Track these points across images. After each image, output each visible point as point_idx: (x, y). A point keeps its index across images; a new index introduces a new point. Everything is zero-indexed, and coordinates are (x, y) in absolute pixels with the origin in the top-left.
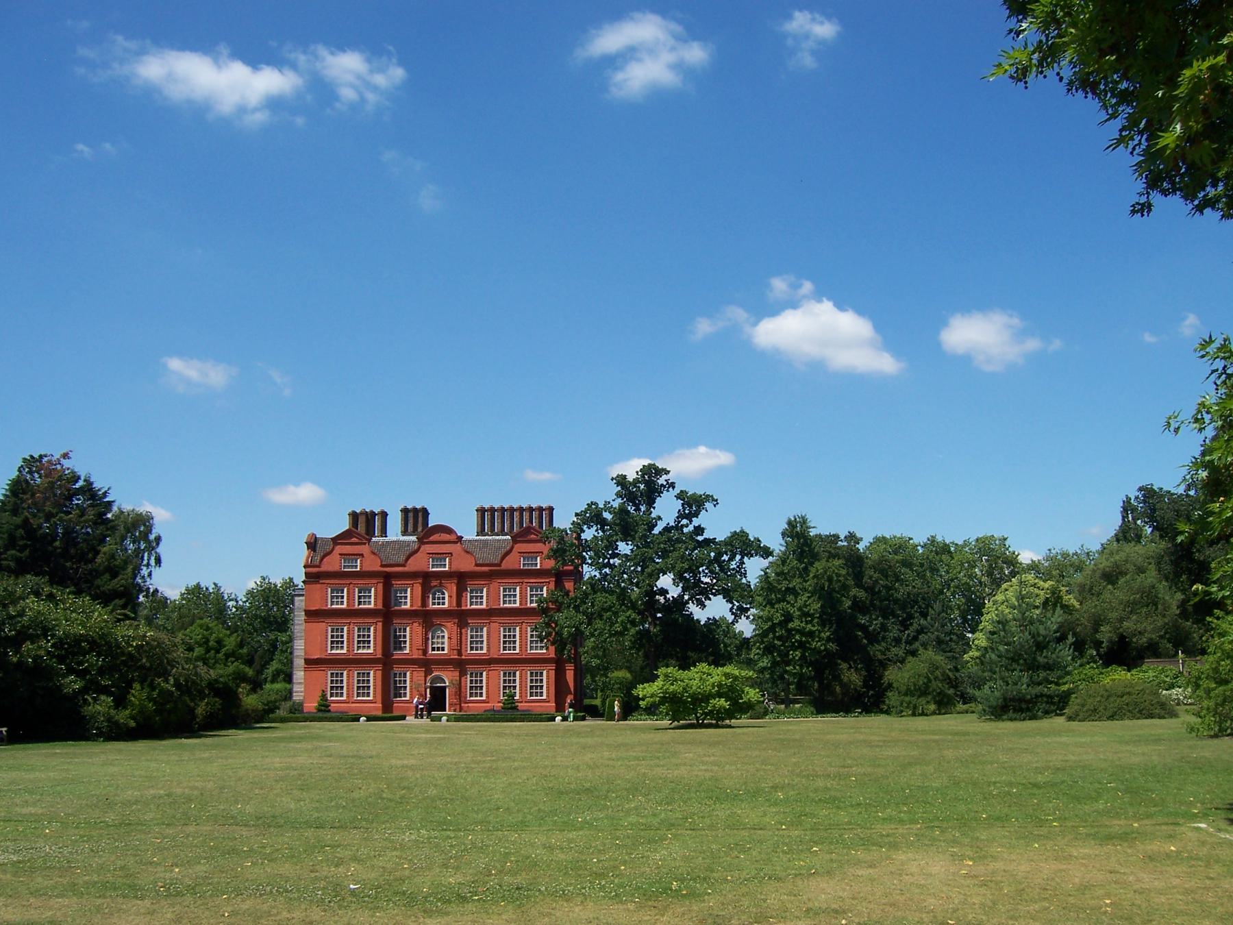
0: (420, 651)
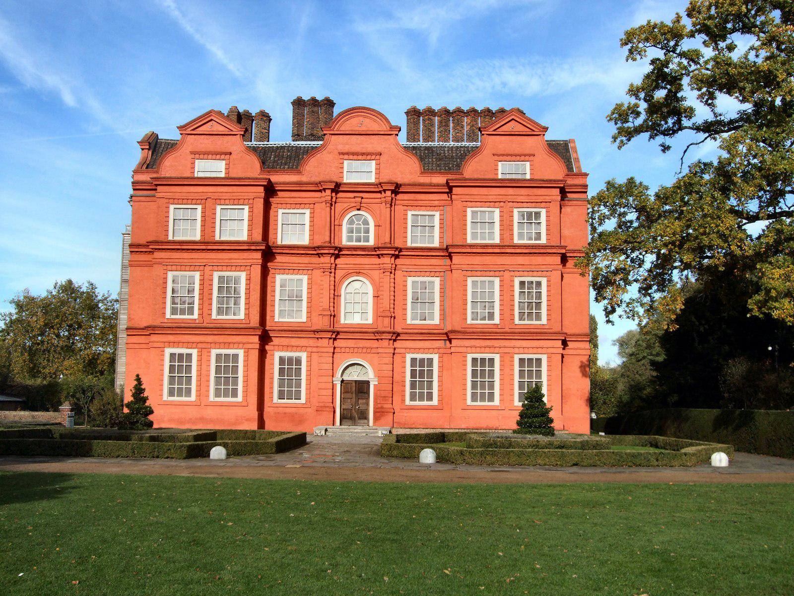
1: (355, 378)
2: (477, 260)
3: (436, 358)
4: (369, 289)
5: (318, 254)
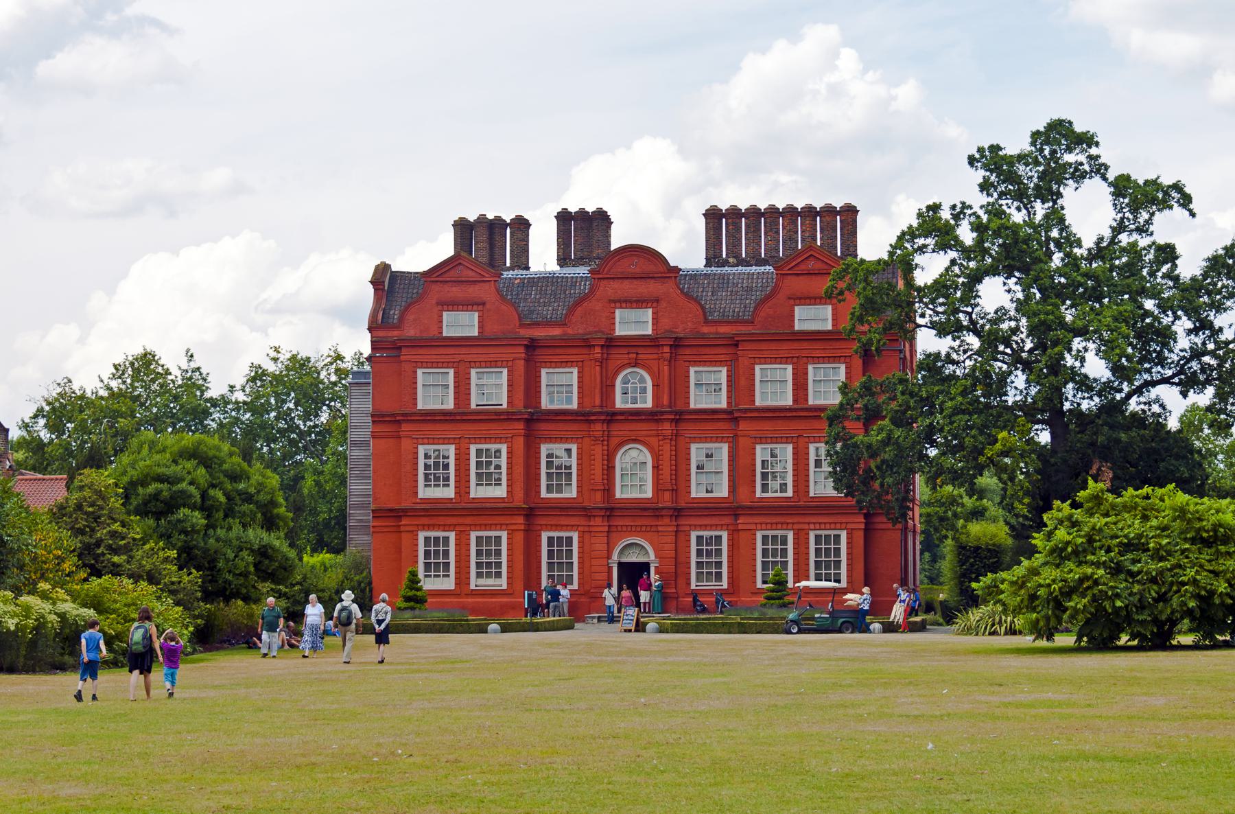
0: (599, 496)
2: (768, 425)
3: (725, 535)
4: (648, 458)
5: (587, 420)
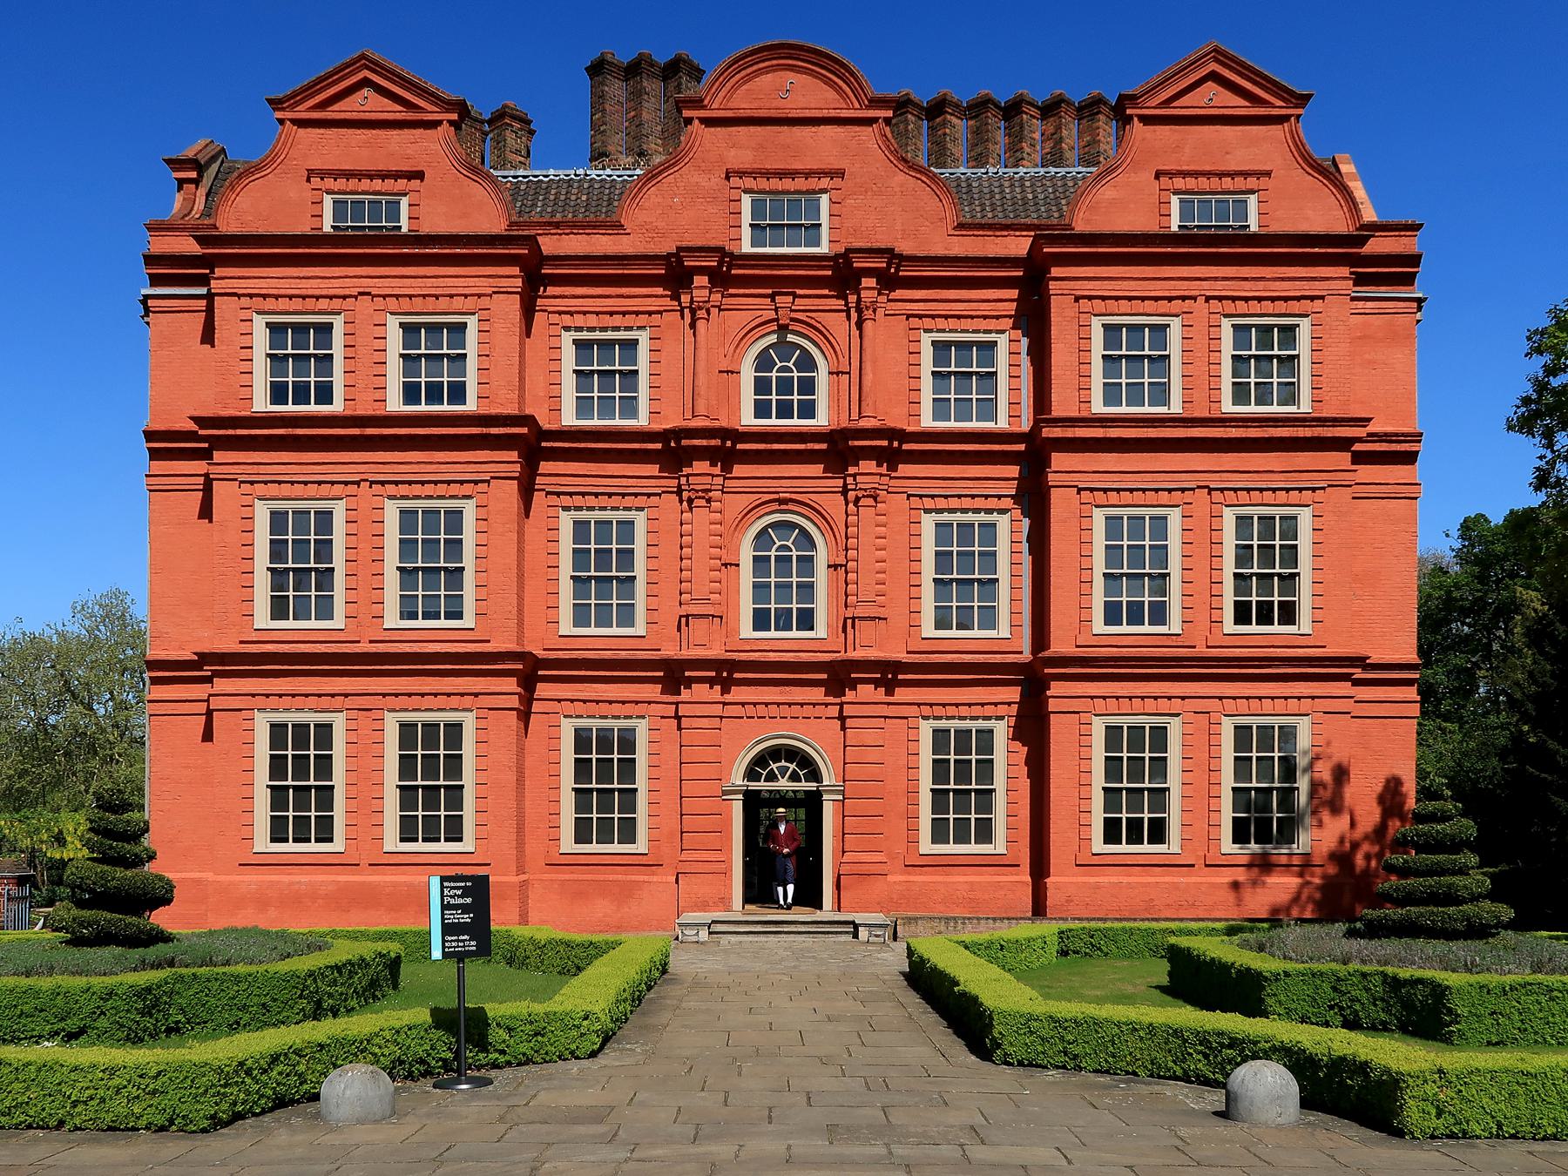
1: (783, 784)
